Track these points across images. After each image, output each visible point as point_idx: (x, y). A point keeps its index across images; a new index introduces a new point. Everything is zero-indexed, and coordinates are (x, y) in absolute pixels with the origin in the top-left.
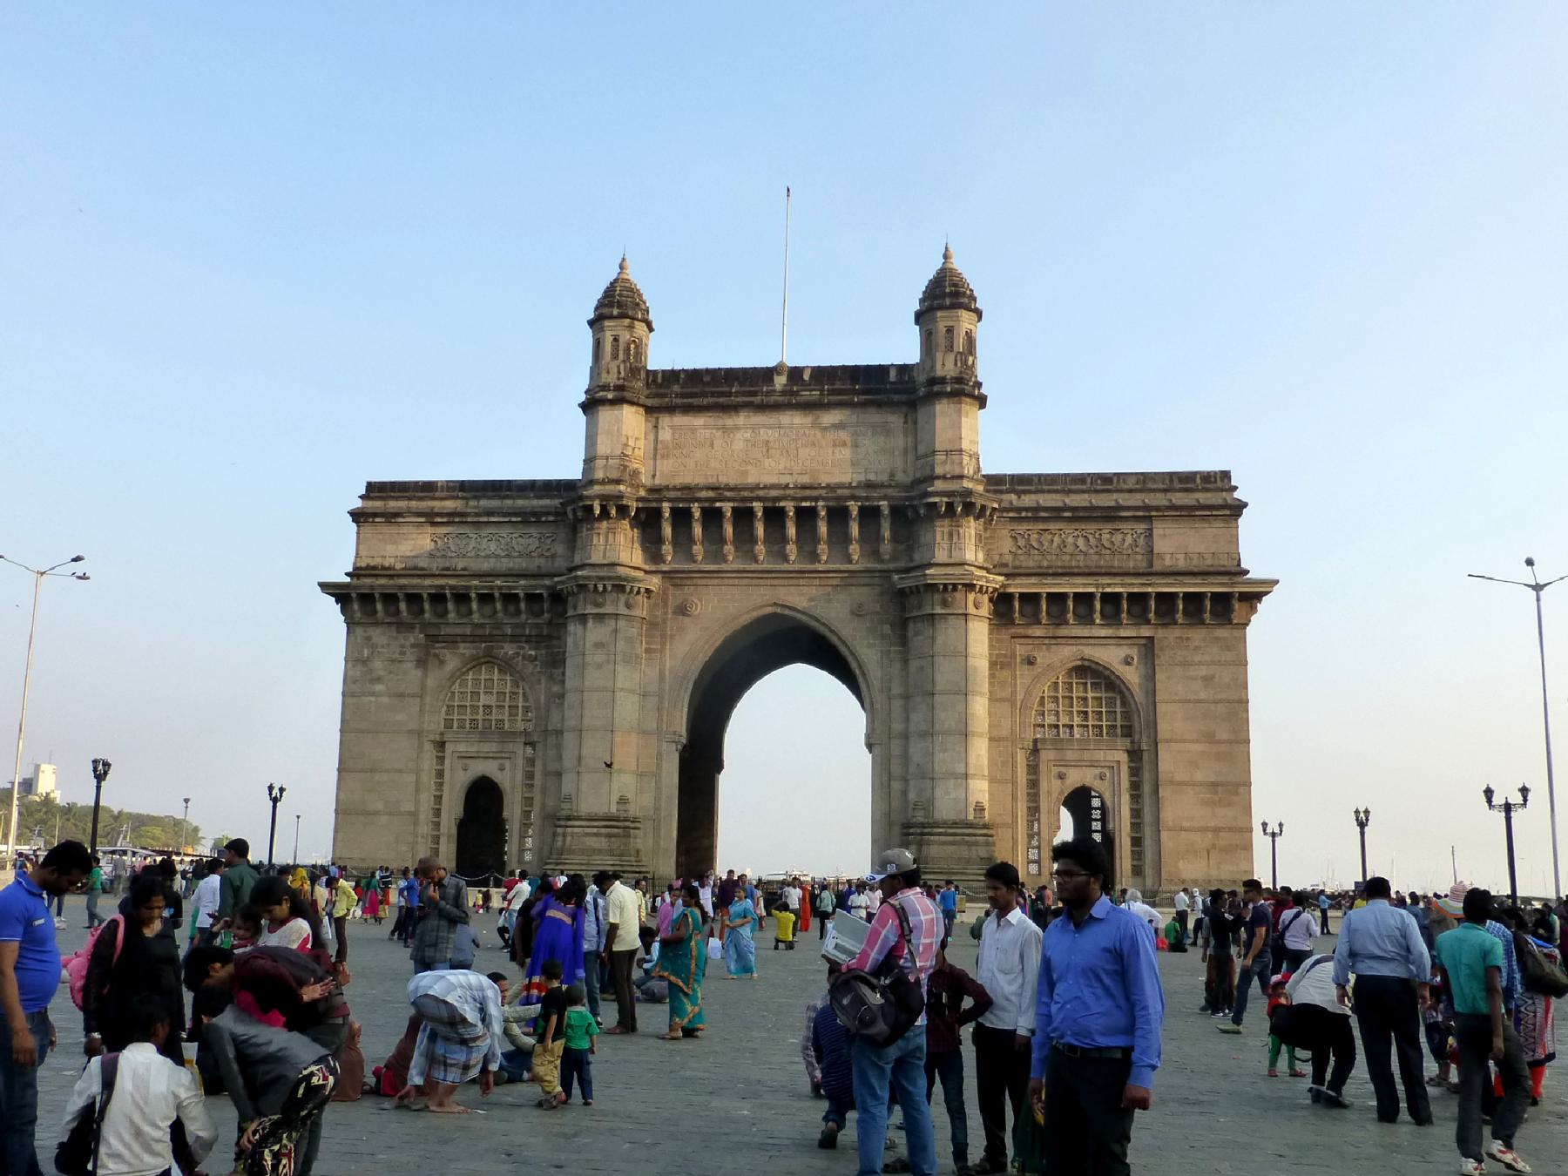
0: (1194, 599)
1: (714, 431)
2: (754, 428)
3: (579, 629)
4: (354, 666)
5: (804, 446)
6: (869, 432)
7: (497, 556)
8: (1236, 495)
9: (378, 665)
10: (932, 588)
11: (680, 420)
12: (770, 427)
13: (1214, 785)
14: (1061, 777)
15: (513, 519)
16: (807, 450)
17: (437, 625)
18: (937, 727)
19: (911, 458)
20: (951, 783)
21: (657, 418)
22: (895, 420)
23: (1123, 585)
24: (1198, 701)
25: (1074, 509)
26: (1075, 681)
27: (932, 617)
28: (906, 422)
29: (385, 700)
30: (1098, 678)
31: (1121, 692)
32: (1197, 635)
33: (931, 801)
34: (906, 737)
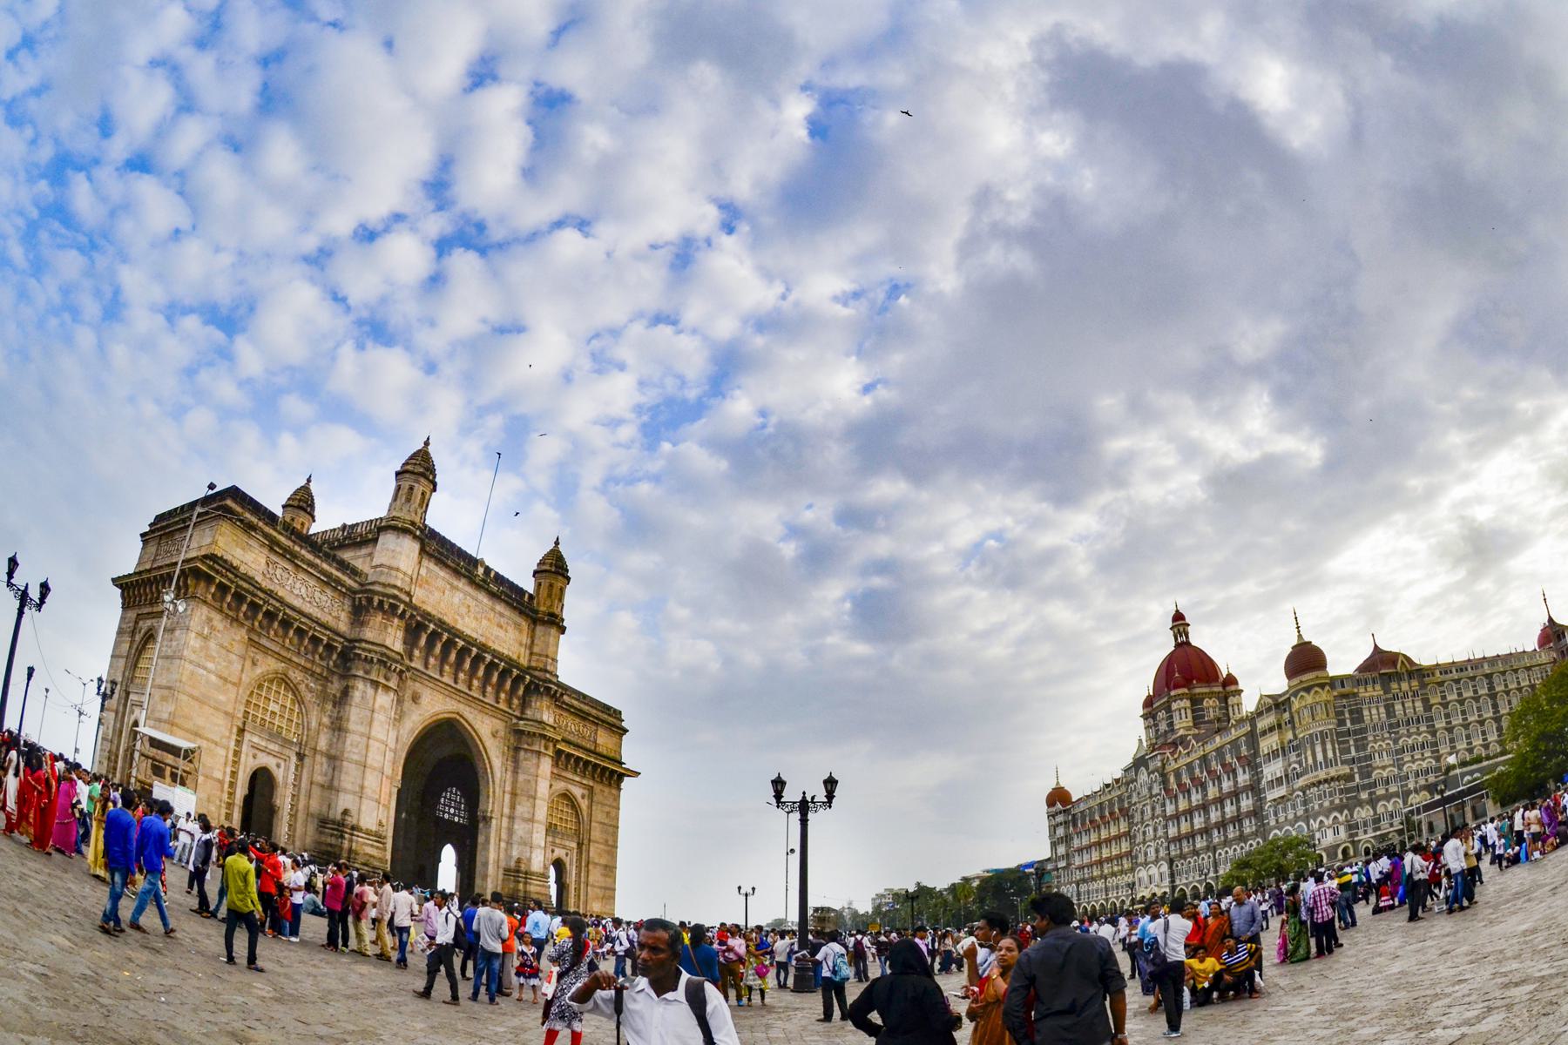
0: (613, 772)
2: (466, 593)
3: (370, 691)
7: (304, 599)
8: (623, 724)
10: (544, 737)
11: (432, 566)
12: (473, 597)
13: (606, 866)
14: (553, 851)
15: (322, 578)
18: (536, 818)
20: (539, 851)
22: (524, 624)
23: (595, 758)
24: (604, 824)
25: (575, 708)
27: (539, 753)
31: (577, 811)
32: (606, 790)
33: (529, 860)
34: (512, 818)
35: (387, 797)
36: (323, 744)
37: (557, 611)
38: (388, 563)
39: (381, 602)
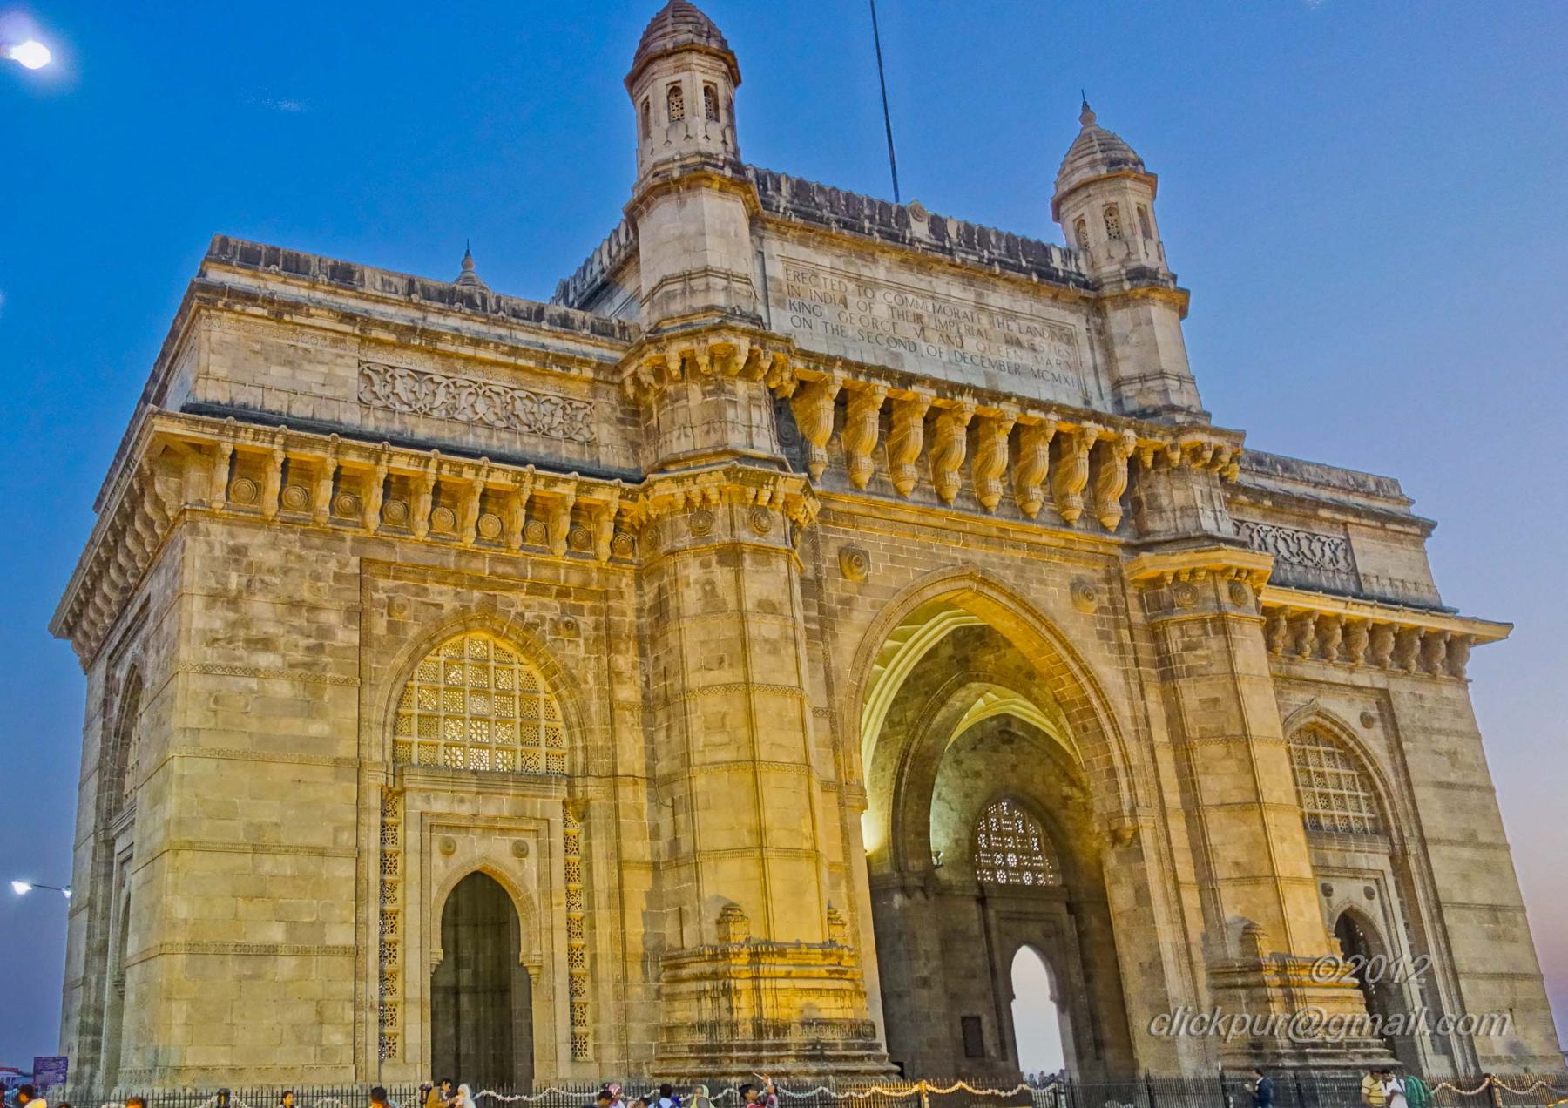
0: (1428, 640)
1: (845, 281)
2: (899, 288)
3: (722, 576)
4: (208, 607)
5: (970, 332)
6: (1046, 335)
9: (260, 606)
13: (1493, 908)
15: (521, 362)
16: (975, 341)
17: (390, 545)
19: (1105, 383)
21: (761, 238)
22: (1076, 322)
24: (1450, 786)
26: (1307, 747)
28: (1088, 329)
29: (283, 689)
30: (1330, 744)
31: (1363, 766)
35: (837, 842)
36: (631, 754)
37: (1150, 261)
38: (677, 270)
39: (687, 362)
